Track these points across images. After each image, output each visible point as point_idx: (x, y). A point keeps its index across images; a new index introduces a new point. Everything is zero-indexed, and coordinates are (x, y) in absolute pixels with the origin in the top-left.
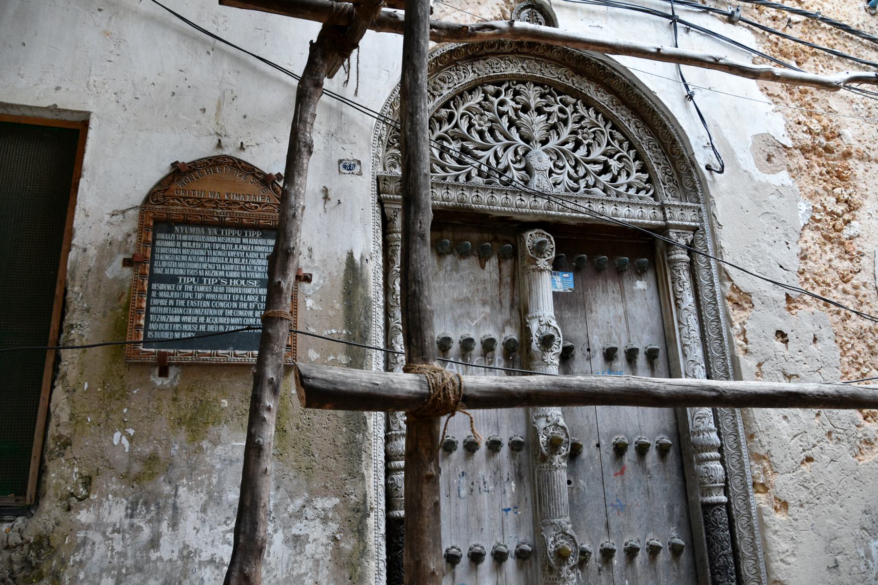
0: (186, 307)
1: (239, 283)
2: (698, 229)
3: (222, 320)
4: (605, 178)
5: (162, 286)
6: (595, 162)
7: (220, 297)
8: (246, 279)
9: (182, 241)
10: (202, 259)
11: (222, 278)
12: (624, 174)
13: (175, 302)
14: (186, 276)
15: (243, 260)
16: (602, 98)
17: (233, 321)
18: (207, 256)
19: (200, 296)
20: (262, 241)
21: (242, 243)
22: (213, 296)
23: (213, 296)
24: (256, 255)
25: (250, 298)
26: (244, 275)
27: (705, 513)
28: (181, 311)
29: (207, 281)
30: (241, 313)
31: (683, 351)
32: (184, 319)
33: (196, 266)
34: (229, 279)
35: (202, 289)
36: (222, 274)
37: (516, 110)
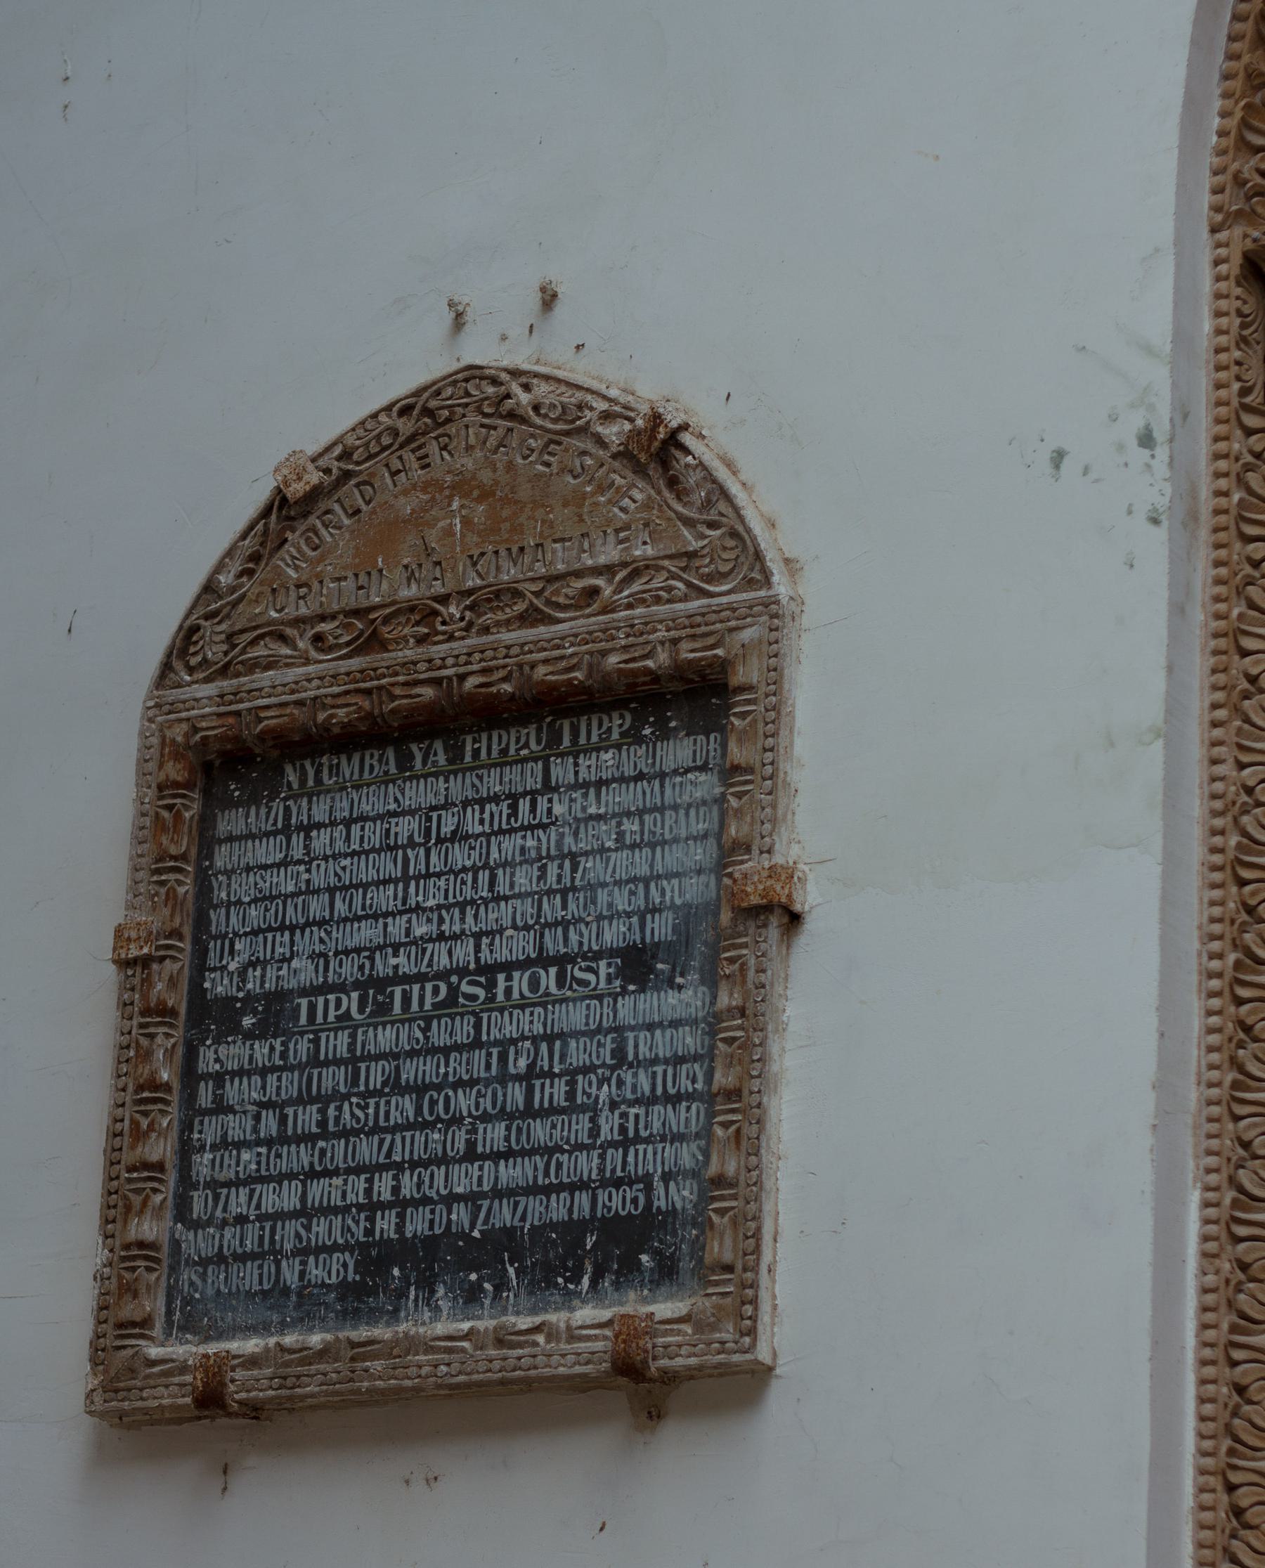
0: (325, 1135)
1: (534, 984)
3: (462, 1179)
5: (234, 1053)
7: (456, 1066)
8: (562, 961)
9: (307, 829)
10: (384, 898)
11: (462, 972)
13: (283, 1120)
14: (324, 989)
15: (552, 870)
17: (510, 1173)
18: (406, 878)
19: (376, 1075)
20: (636, 759)
21: (548, 787)
22: (427, 1069)
23: (427, 1069)
24: (606, 833)
25: (577, 1054)
26: (553, 942)
28: (303, 1157)
29: (406, 999)
30: (540, 1131)
32: (316, 1190)
33: (367, 933)
34: (489, 971)
35: (385, 1038)
36: (464, 952)
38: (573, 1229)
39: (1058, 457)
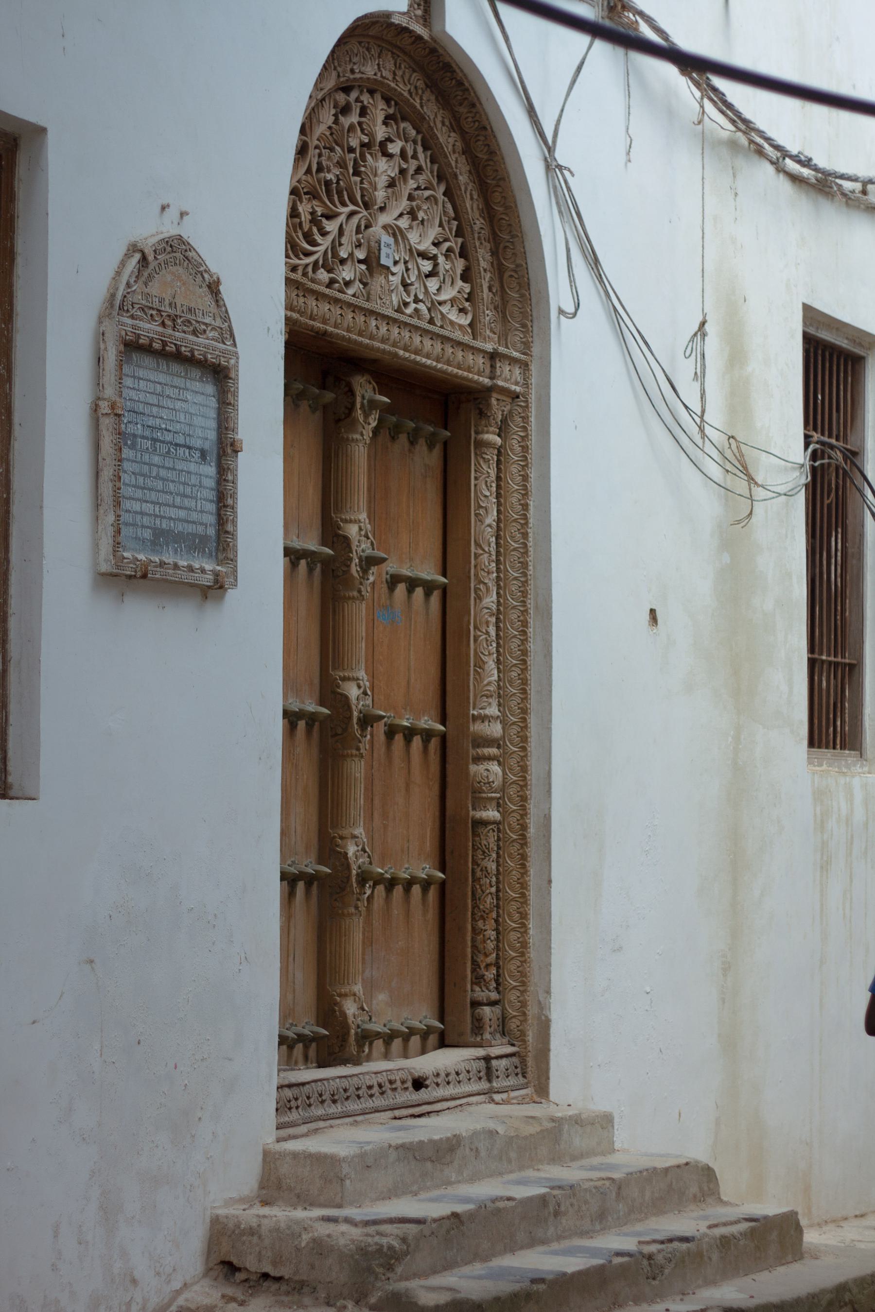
2: (518, 397)
4: (433, 284)
6: (423, 255)
12: (448, 281)
16: (447, 140)
17: (182, 514)
27: (475, 834)
30: (187, 502)
31: (476, 590)
36: (169, 437)
37: (363, 145)
38: (195, 535)
39: (269, 329)
